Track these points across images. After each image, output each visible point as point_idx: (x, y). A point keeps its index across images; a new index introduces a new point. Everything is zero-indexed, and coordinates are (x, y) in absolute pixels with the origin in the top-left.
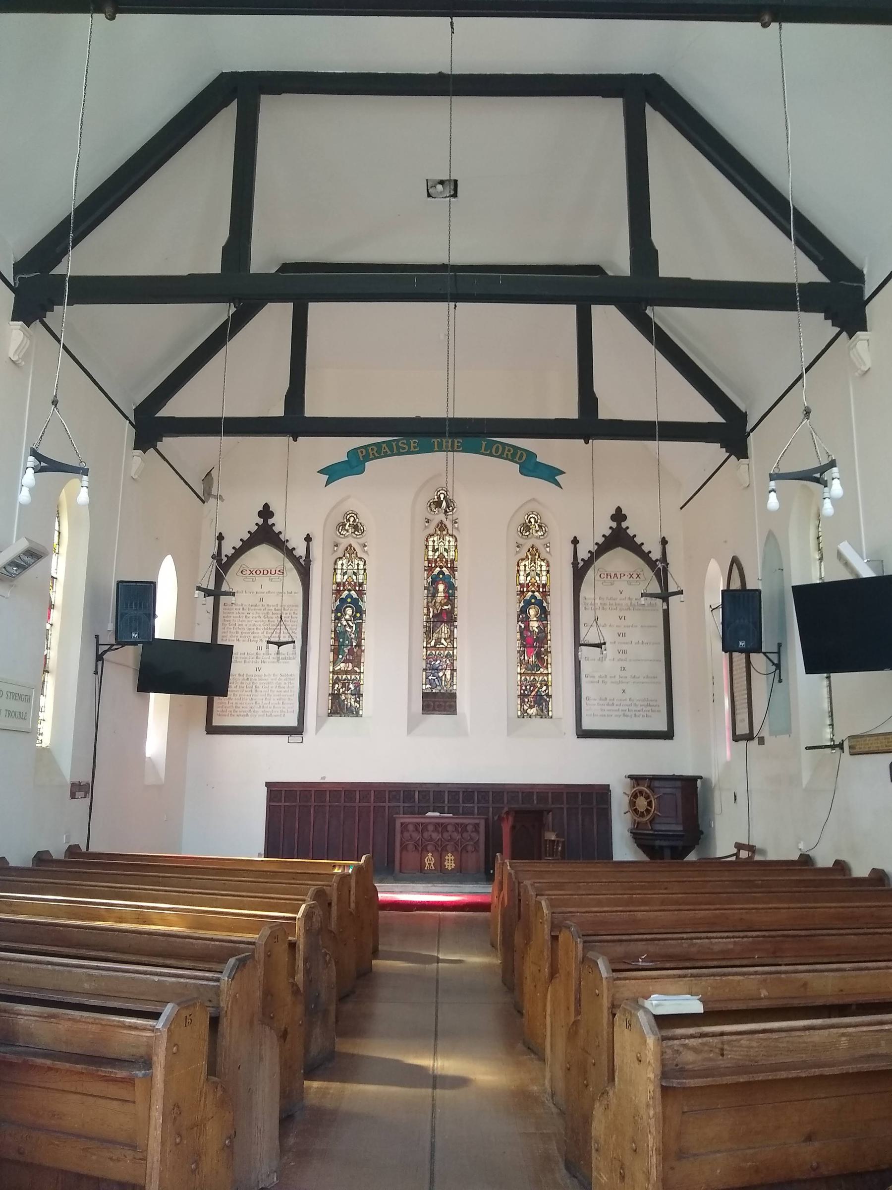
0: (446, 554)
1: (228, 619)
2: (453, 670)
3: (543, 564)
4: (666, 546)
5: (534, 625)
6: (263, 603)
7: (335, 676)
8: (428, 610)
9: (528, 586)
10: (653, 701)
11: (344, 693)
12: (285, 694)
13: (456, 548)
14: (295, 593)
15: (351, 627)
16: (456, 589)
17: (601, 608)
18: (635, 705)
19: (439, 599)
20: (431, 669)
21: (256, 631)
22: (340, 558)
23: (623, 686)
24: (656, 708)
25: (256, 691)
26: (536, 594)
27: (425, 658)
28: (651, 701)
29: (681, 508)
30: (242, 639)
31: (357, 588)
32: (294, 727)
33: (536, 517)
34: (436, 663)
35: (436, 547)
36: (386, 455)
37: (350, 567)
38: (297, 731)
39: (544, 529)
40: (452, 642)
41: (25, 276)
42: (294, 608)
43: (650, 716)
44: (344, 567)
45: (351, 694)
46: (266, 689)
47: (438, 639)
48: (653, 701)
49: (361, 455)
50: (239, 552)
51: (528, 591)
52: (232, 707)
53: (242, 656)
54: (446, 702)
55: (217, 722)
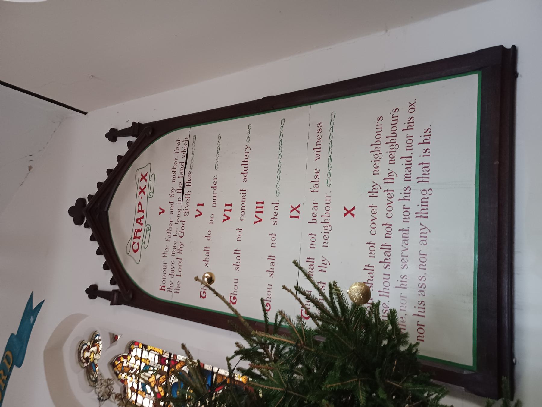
10: (379, 127)
17: (179, 256)
18: (389, 179)
23: (336, 213)
24: (403, 117)
28: (378, 133)
29: (85, 113)
48: (379, 127)
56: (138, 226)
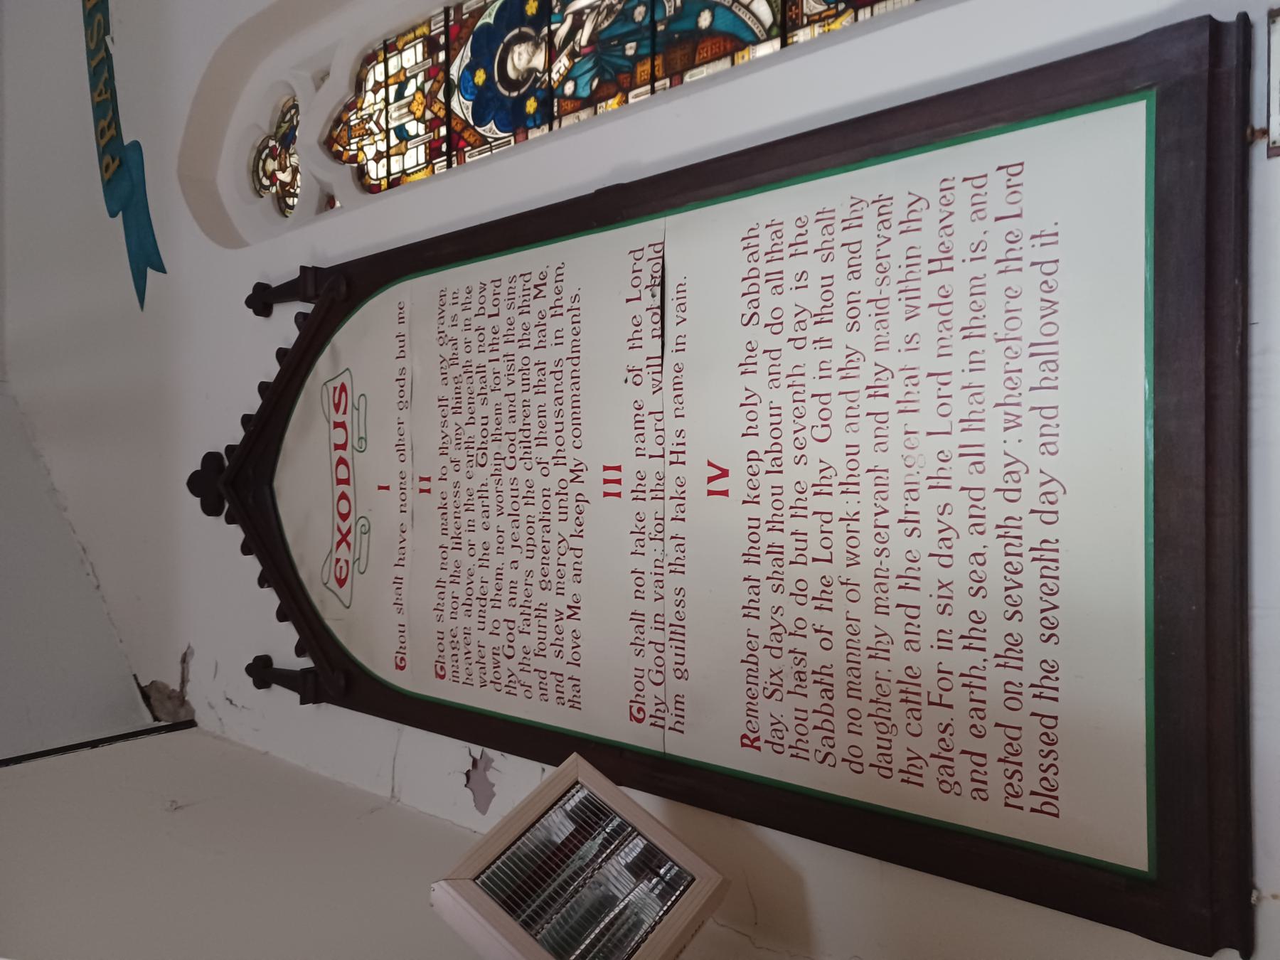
6: (435, 476)
14: (401, 320)
21: (536, 511)
30: (570, 587)
42: (450, 311)
46: (838, 405)
52: (972, 680)
53: (649, 590)
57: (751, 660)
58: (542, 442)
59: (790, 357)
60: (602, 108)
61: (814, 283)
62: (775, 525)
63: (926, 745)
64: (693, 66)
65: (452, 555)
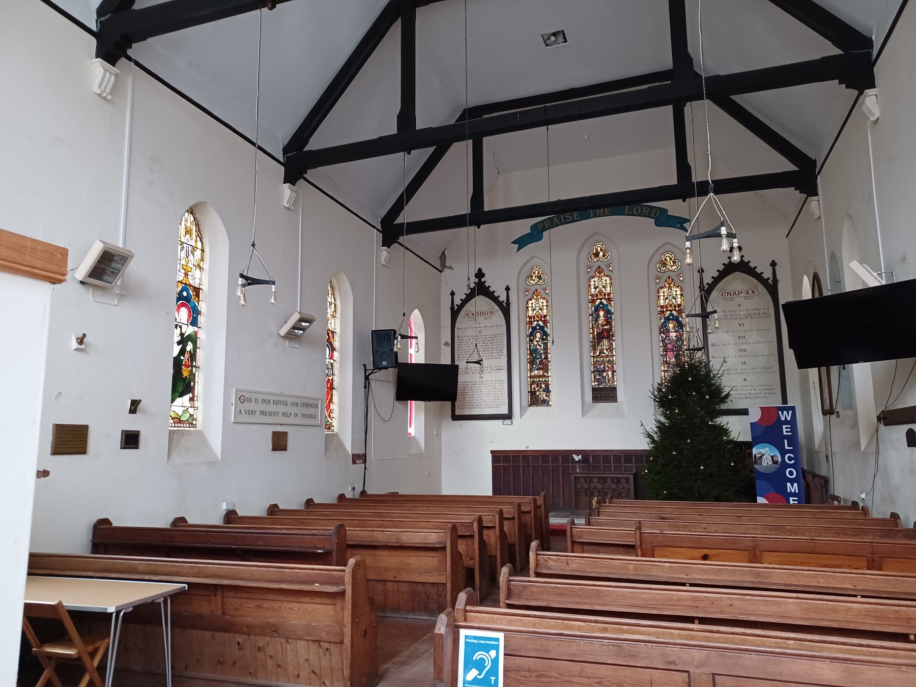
0: (604, 289)
1: (461, 346)
2: (613, 371)
3: (678, 289)
4: (776, 267)
5: (673, 335)
7: (532, 380)
8: (593, 330)
9: (667, 307)
10: (768, 386)
11: (538, 390)
12: (499, 393)
13: (611, 285)
14: (501, 326)
15: (540, 346)
16: (613, 314)
19: (600, 322)
20: (598, 372)
22: (531, 299)
23: (744, 376)
25: (480, 392)
26: (674, 312)
27: (593, 364)
29: (787, 236)
31: (543, 319)
32: (507, 414)
33: (671, 256)
34: (601, 367)
35: (596, 285)
36: (557, 225)
37: (537, 305)
38: (508, 416)
39: (677, 264)
40: (611, 351)
41: (289, 155)
42: (501, 336)
43: (767, 397)
44: (533, 305)
45: (544, 391)
47: (602, 349)
49: (540, 228)
50: (465, 302)
51: (667, 311)
52: (466, 403)
53: (471, 369)
54: (609, 394)
55: (458, 413)
56: (732, 293)
57: (465, 382)
58: (485, 353)
59: (492, 385)
60: (529, 351)
61: (498, 387)
62: (477, 384)
63: (461, 399)
64: (530, 364)
65: (471, 338)
